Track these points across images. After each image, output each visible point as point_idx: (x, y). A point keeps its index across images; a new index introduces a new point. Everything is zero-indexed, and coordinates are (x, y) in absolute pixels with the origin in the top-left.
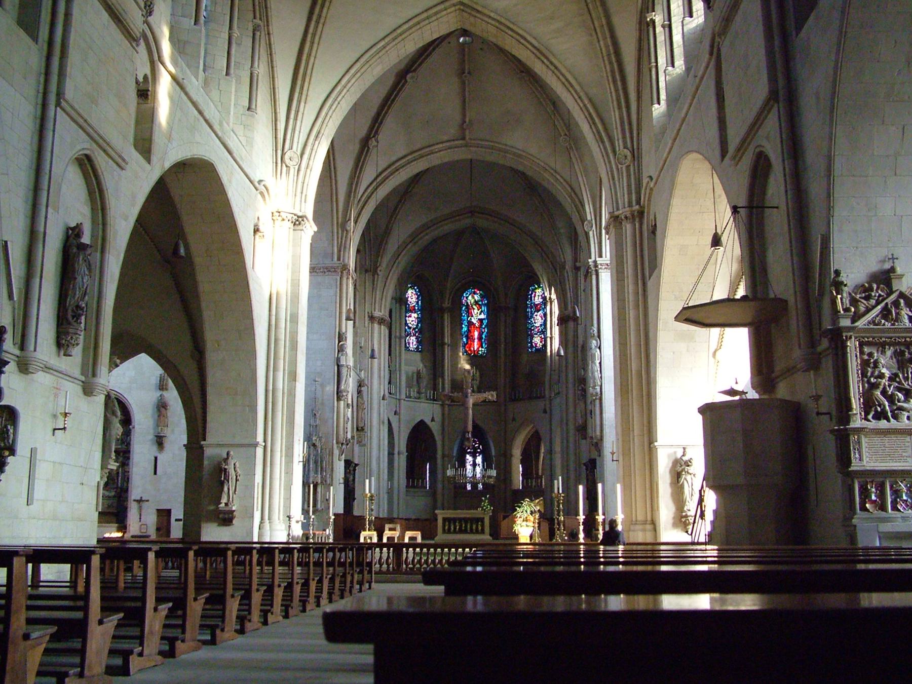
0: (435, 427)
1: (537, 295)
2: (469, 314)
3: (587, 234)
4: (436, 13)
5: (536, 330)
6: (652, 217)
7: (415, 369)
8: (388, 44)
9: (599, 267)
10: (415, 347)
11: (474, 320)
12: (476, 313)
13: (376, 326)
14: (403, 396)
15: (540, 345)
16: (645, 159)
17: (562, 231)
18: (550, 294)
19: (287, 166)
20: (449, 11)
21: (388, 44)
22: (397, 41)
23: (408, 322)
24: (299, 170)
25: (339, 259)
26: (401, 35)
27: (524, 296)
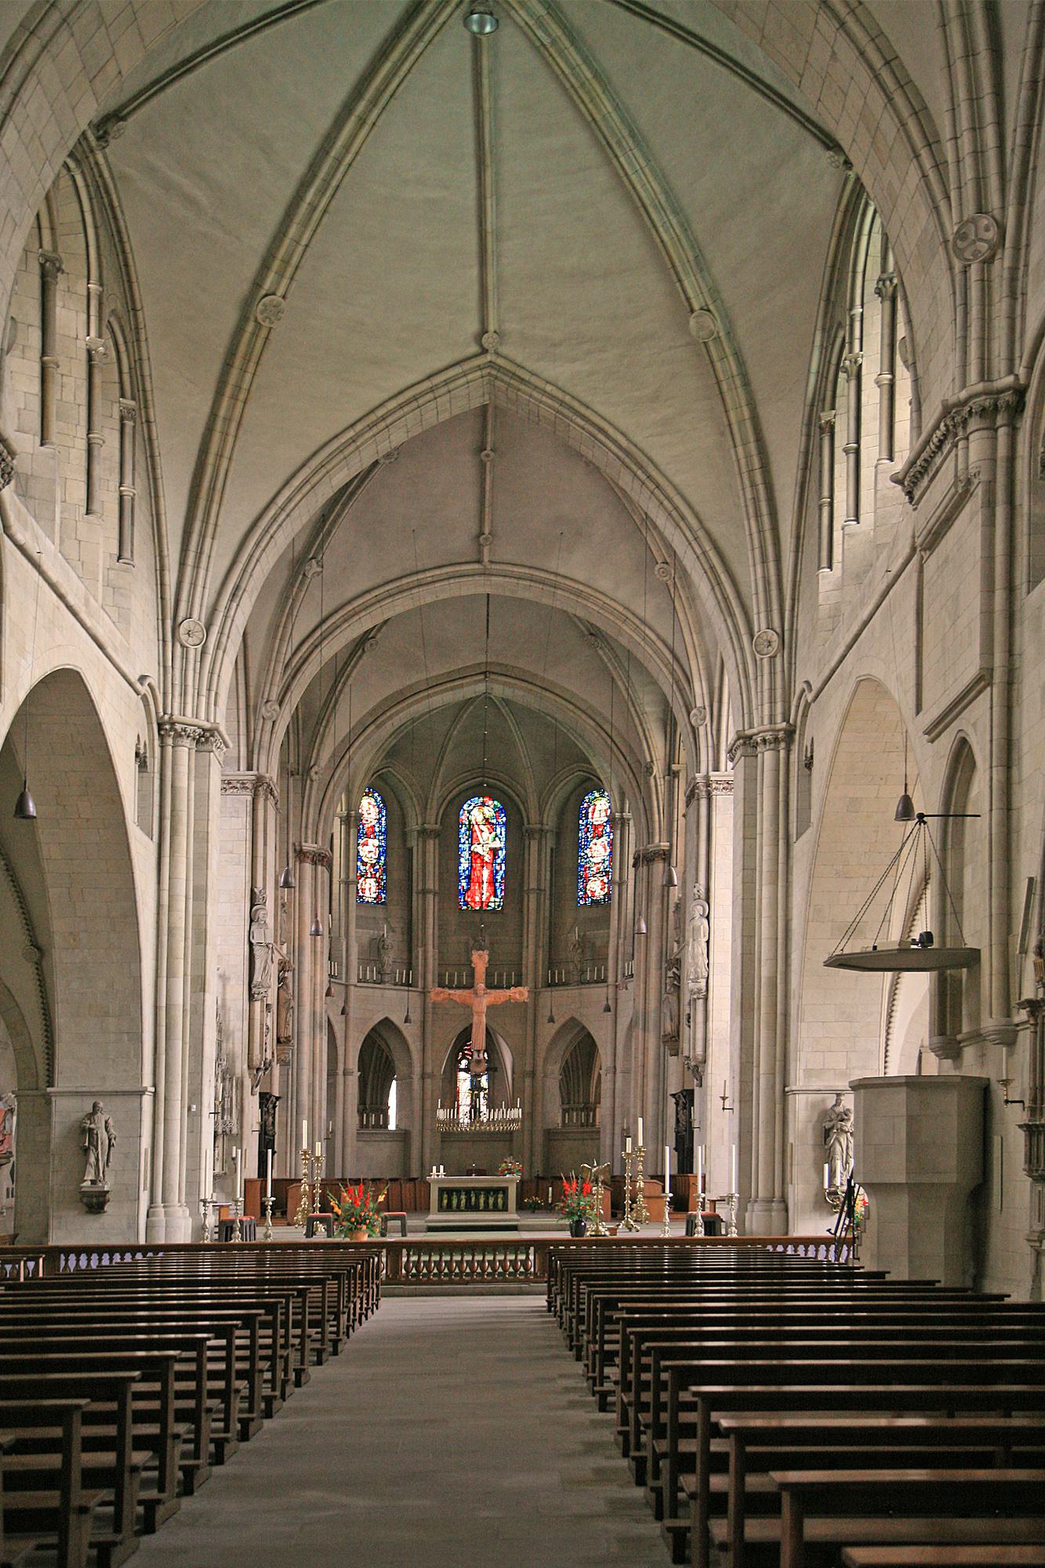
1: (597, 808)
2: (472, 838)
3: (694, 731)
4: (446, 383)
5: (594, 869)
6: (807, 742)
8: (358, 435)
9: (714, 786)
10: (374, 896)
12: (485, 838)
13: (308, 867)
16: (802, 652)
17: (647, 709)
18: (622, 812)
19: (182, 646)
20: (470, 377)
21: (358, 435)
22: (375, 430)
23: (361, 854)
24: (203, 652)
25: (250, 768)
26: (383, 418)
27: (573, 810)
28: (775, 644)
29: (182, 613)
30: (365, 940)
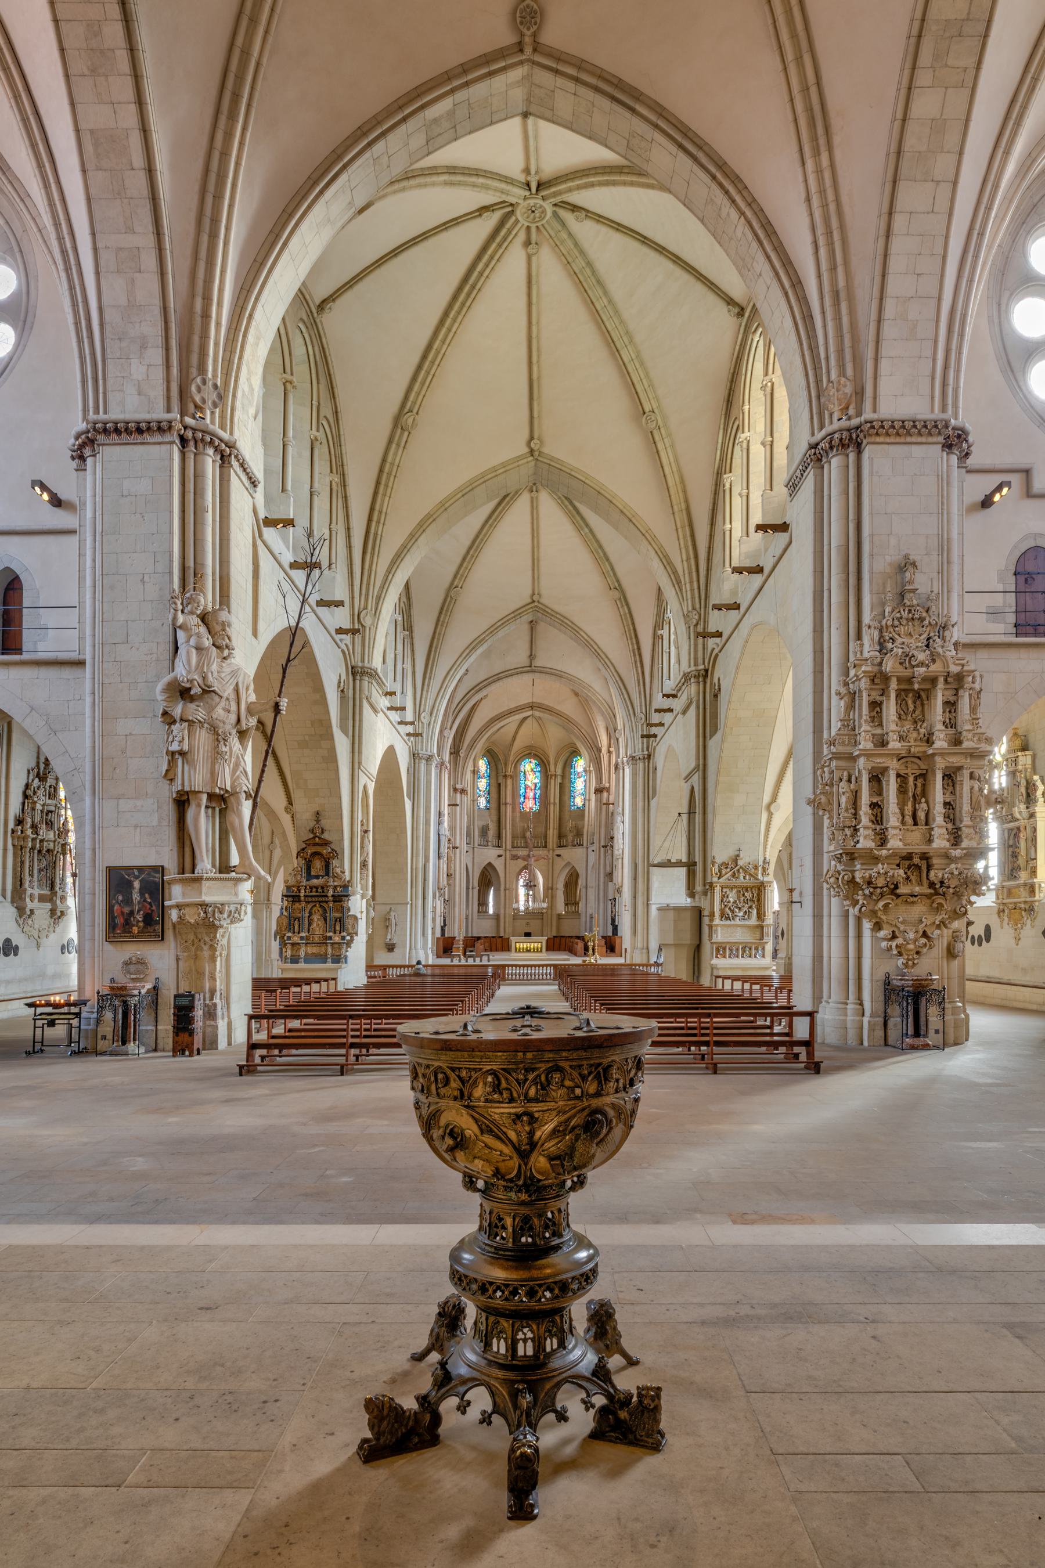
0: (499, 865)
7: (484, 823)
11: (529, 783)
13: (458, 795)
14: (476, 845)
15: (580, 804)
27: (568, 765)
28: (644, 719)
29: (422, 710)
30: (481, 826)
